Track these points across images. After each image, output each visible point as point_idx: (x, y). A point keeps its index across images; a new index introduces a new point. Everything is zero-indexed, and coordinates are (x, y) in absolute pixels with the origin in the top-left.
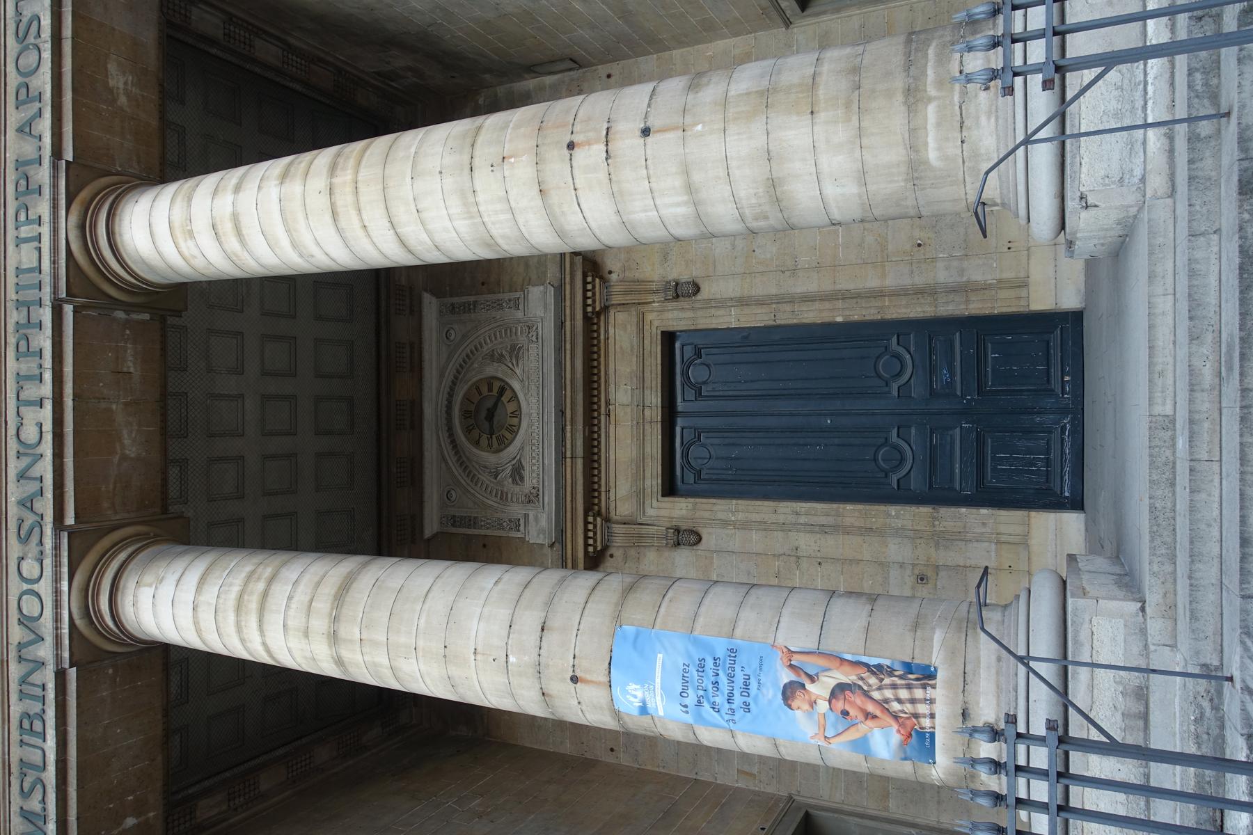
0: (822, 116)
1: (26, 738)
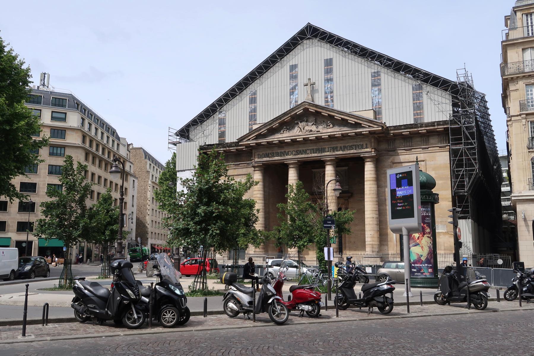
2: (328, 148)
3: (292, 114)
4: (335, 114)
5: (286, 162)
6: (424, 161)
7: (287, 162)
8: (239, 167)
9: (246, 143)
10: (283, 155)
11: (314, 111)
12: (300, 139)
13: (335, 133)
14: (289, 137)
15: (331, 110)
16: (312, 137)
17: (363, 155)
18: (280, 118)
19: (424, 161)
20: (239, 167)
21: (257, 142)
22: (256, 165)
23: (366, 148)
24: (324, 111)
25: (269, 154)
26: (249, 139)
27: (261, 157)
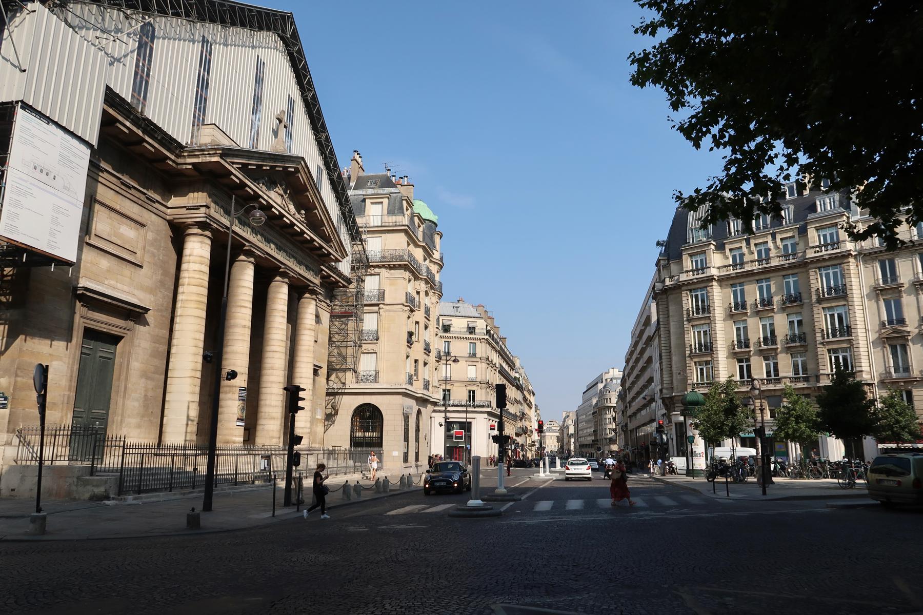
8: (128, 195)
15: (319, 198)
20: (128, 195)
26: (233, 163)
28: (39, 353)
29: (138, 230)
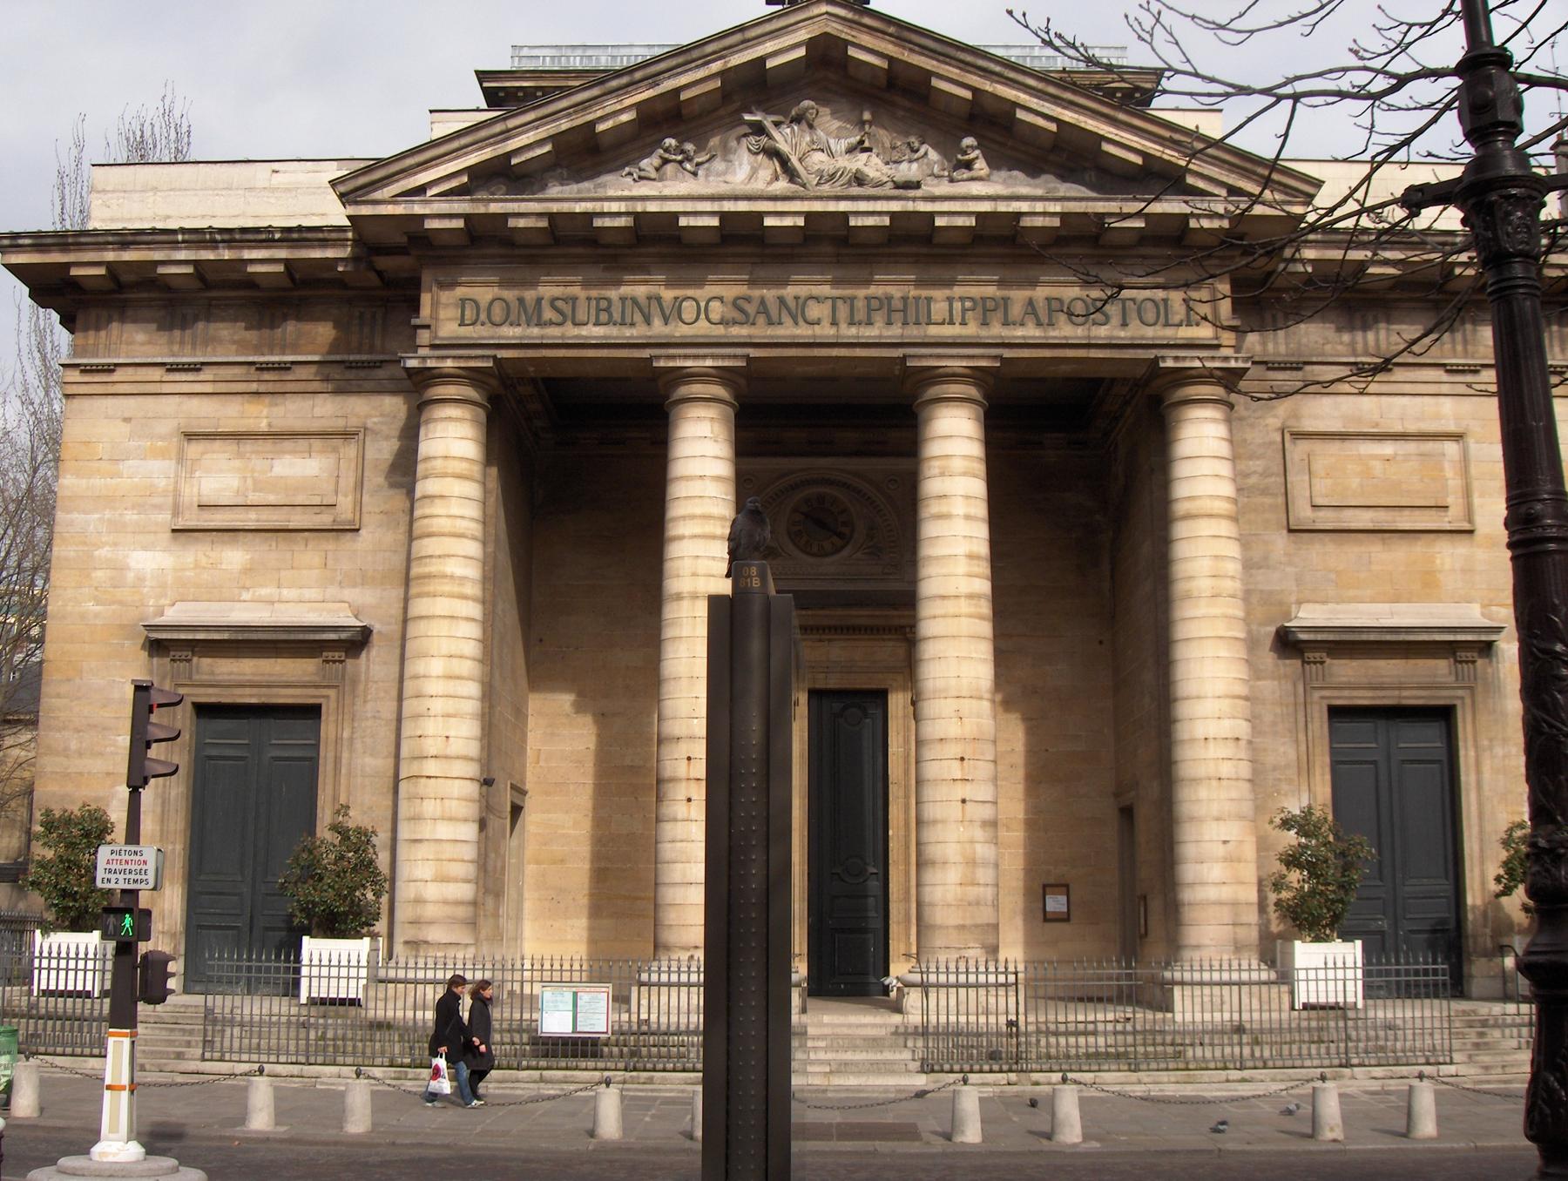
0: (959, 889)
1: (594, 303)
2: (950, 300)
3: (736, 60)
4: (1023, 98)
5: (662, 363)
6: (1457, 437)
7: (671, 364)
9: (399, 210)
10: (638, 317)
11: (885, 65)
12: (788, 222)
13: (1024, 207)
14: (712, 198)
15: (998, 69)
16: (870, 214)
17: (1176, 358)
18: (653, 80)
19: (1457, 437)
21: (481, 209)
22: (449, 363)
23: (1189, 325)
24: (953, 72)
25: (539, 300)
26: (421, 190)
27: (483, 316)
28: (81, 774)
29: (335, 450)
